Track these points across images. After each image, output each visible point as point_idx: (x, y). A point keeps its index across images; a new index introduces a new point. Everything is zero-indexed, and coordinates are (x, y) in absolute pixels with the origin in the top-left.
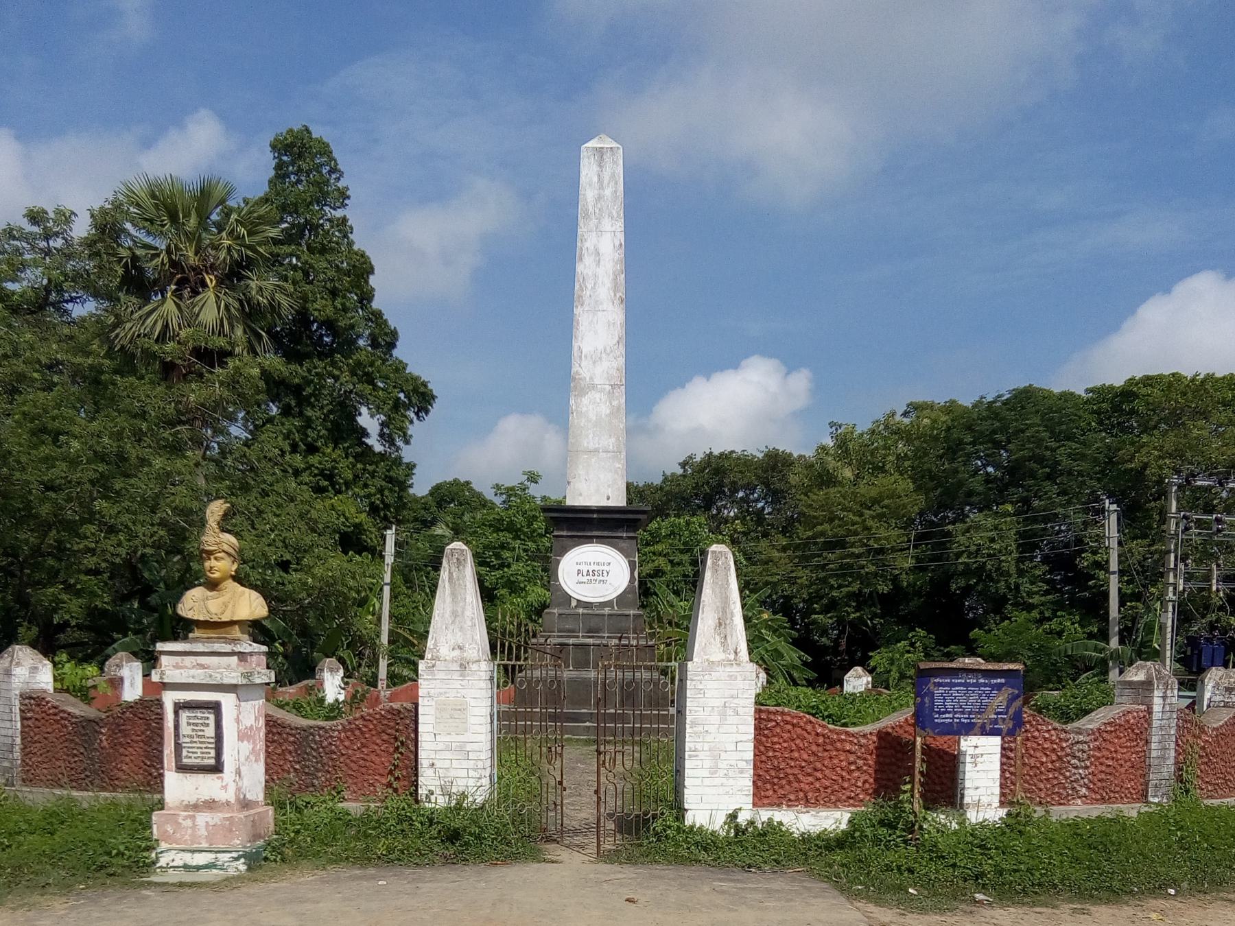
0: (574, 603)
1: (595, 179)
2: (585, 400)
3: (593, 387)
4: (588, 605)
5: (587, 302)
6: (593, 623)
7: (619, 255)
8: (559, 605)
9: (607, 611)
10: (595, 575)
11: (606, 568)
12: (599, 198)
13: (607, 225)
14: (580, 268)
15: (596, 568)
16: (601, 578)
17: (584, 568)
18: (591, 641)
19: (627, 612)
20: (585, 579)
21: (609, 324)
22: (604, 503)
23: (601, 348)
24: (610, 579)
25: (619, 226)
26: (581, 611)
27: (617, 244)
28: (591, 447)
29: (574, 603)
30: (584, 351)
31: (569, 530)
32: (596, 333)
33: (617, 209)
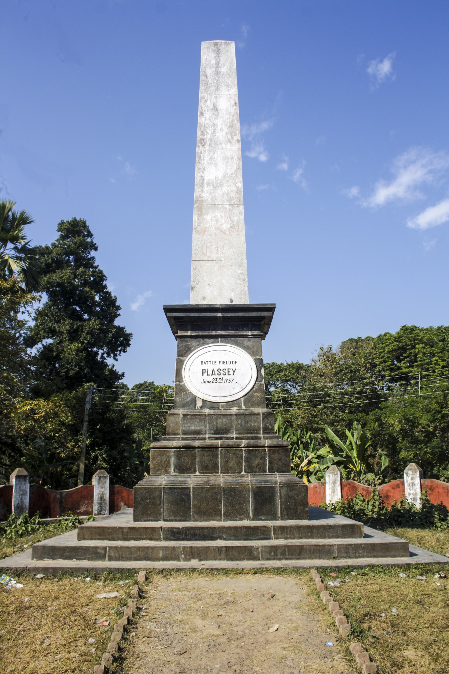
0: (199, 404)
1: (213, 62)
2: (208, 217)
3: (214, 206)
4: (213, 405)
5: (208, 143)
6: (221, 422)
7: (235, 110)
8: (184, 406)
9: (234, 410)
10: (222, 374)
11: (232, 366)
12: (218, 73)
13: (223, 91)
14: (201, 120)
15: (222, 367)
16: (227, 377)
17: (210, 367)
18: (219, 442)
19: (256, 411)
20: (210, 378)
21: (226, 159)
22: (228, 303)
23: (220, 175)
24: (237, 378)
25: (234, 91)
26: (207, 411)
27: (233, 102)
28: (214, 256)
29: (199, 404)
30: (206, 179)
31: (192, 330)
32: (216, 164)
33: (233, 80)
